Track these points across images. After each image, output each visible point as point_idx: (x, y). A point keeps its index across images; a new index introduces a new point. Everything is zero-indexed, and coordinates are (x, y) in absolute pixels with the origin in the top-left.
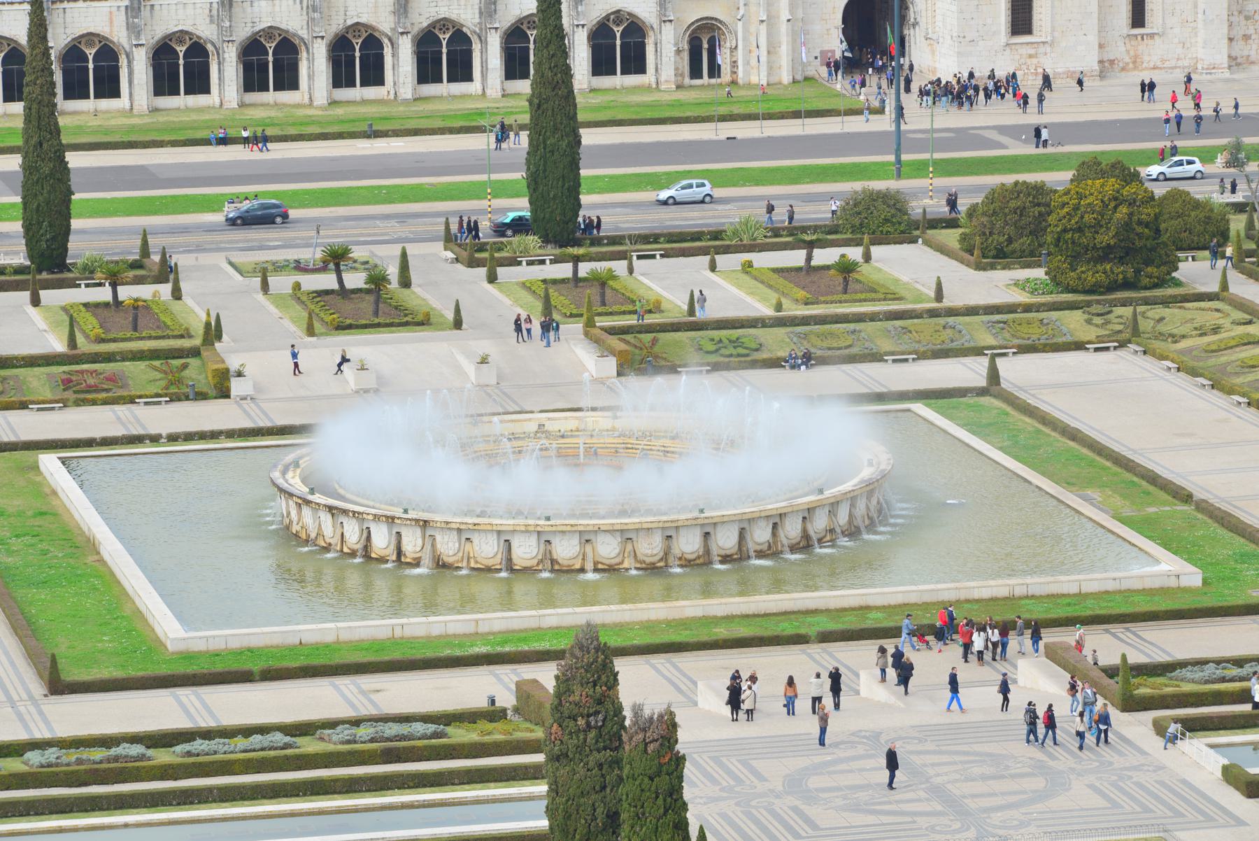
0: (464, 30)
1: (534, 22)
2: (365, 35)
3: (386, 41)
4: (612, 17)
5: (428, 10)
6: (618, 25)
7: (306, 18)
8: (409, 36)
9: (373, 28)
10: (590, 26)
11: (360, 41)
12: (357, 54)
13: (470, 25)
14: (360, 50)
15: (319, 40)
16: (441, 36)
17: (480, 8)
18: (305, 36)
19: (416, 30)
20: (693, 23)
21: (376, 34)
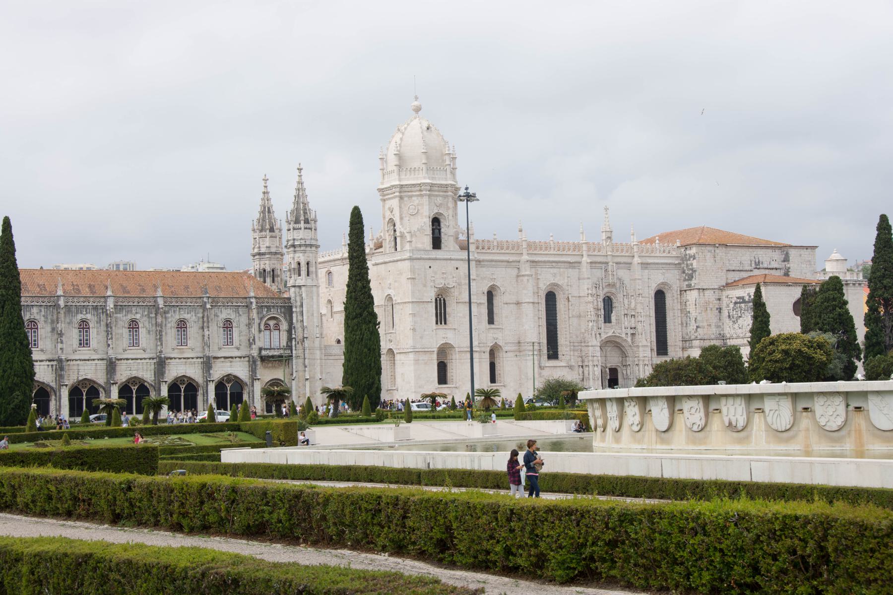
0: (146, 384)
1: (184, 380)
2: (89, 386)
3: (101, 390)
4: (225, 378)
5: (126, 372)
6: (228, 383)
7: (55, 375)
8: (117, 385)
9: (94, 382)
10: (216, 381)
11: (86, 390)
12: (84, 397)
13: (149, 381)
14: (86, 395)
15: (64, 387)
16: (133, 388)
17: (155, 372)
18: (54, 386)
19: (119, 383)
20: (268, 382)
21: (96, 386)
